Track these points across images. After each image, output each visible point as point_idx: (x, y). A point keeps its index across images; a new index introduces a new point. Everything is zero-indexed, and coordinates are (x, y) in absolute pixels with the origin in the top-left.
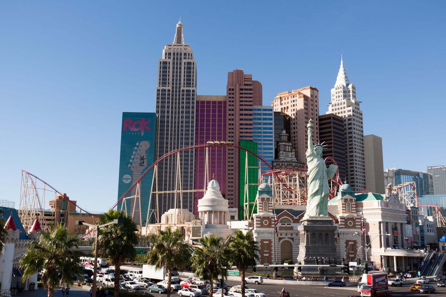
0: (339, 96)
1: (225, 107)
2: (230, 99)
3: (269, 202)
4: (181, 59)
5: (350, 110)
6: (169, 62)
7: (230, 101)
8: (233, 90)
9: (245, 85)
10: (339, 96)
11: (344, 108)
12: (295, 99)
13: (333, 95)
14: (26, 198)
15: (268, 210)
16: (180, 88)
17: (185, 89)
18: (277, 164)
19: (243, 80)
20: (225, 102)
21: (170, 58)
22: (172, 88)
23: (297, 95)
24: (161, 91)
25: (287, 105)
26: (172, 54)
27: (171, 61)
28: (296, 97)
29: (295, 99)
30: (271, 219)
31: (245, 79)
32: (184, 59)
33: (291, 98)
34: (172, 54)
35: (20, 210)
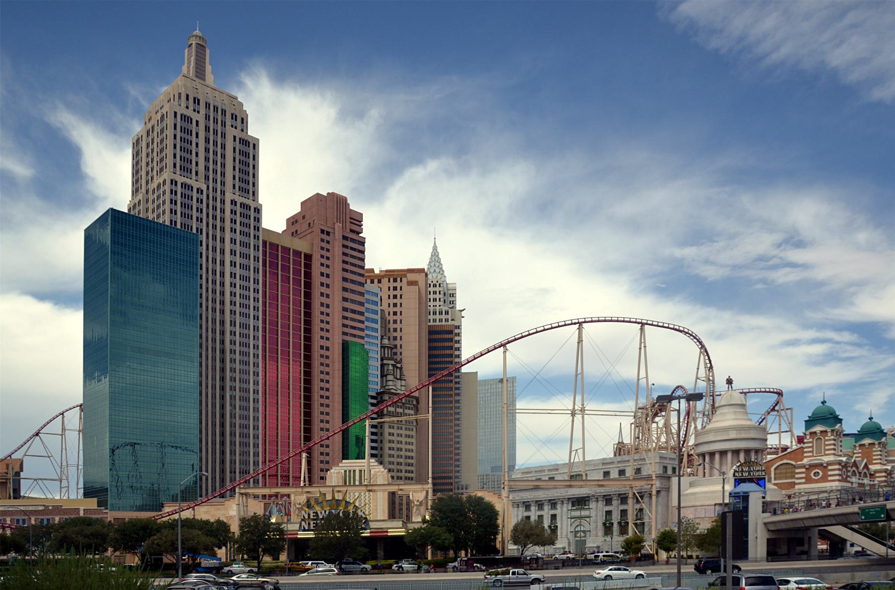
4: (224, 124)
6: (197, 122)
15: (824, 452)
19: (348, 220)
26: (202, 104)
27: (201, 117)
28: (401, 281)
29: (398, 284)
31: (351, 218)
32: (232, 126)
33: (389, 282)
34: (202, 104)
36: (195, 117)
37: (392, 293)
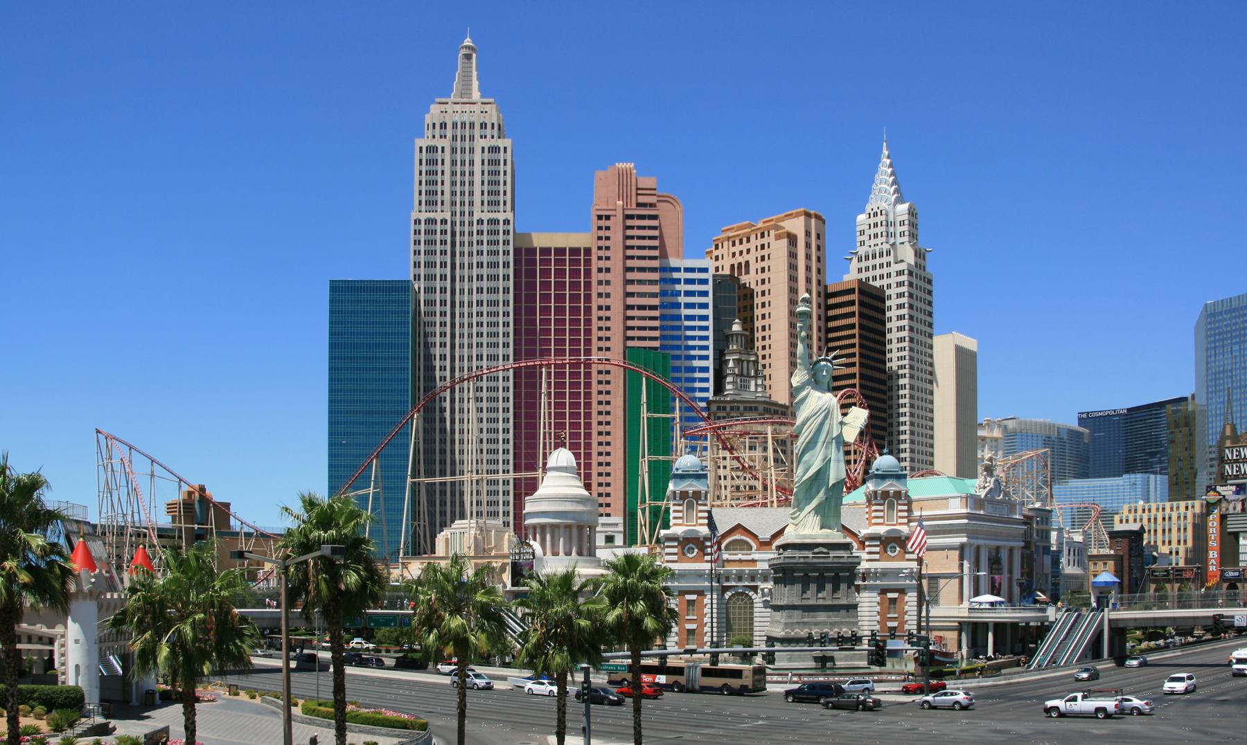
0: (876, 236)
1: (588, 262)
2: (601, 243)
3: (700, 502)
5: (902, 269)
6: (443, 148)
7: (600, 248)
8: (608, 218)
9: (639, 205)
10: (876, 236)
11: (889, 264)
12: (765, 241)
13: (862, 233)
14: (111, 496)
16: (471, 214)
17: (486, 216)
18: (719, 408)
20: (588, 251)
21: (443, 137)
22: (452, 215)
23: (772, 233)
24: (423, 222)
25: (746, 257)
26: (449, 126)
28: (769, 235)
29: (765, 241)
30: (703, 543)
32: (481, 137)
34: (449, 126)
35: (102, 526)
36: (439, 143)
37: (760, 253)
